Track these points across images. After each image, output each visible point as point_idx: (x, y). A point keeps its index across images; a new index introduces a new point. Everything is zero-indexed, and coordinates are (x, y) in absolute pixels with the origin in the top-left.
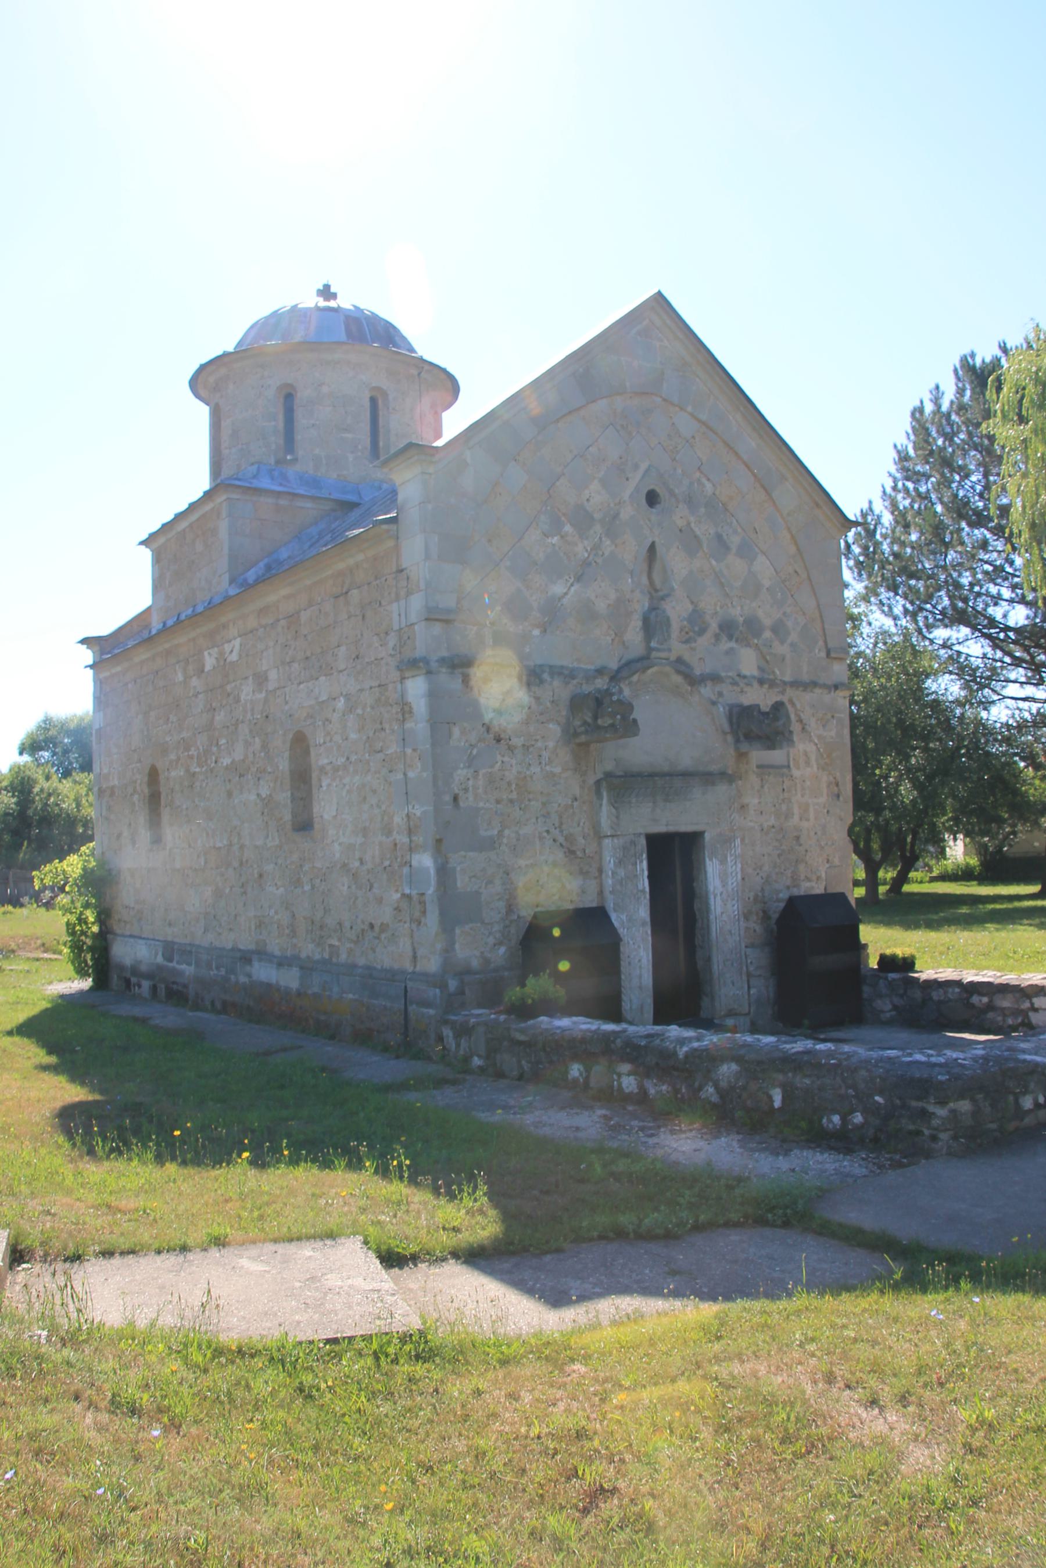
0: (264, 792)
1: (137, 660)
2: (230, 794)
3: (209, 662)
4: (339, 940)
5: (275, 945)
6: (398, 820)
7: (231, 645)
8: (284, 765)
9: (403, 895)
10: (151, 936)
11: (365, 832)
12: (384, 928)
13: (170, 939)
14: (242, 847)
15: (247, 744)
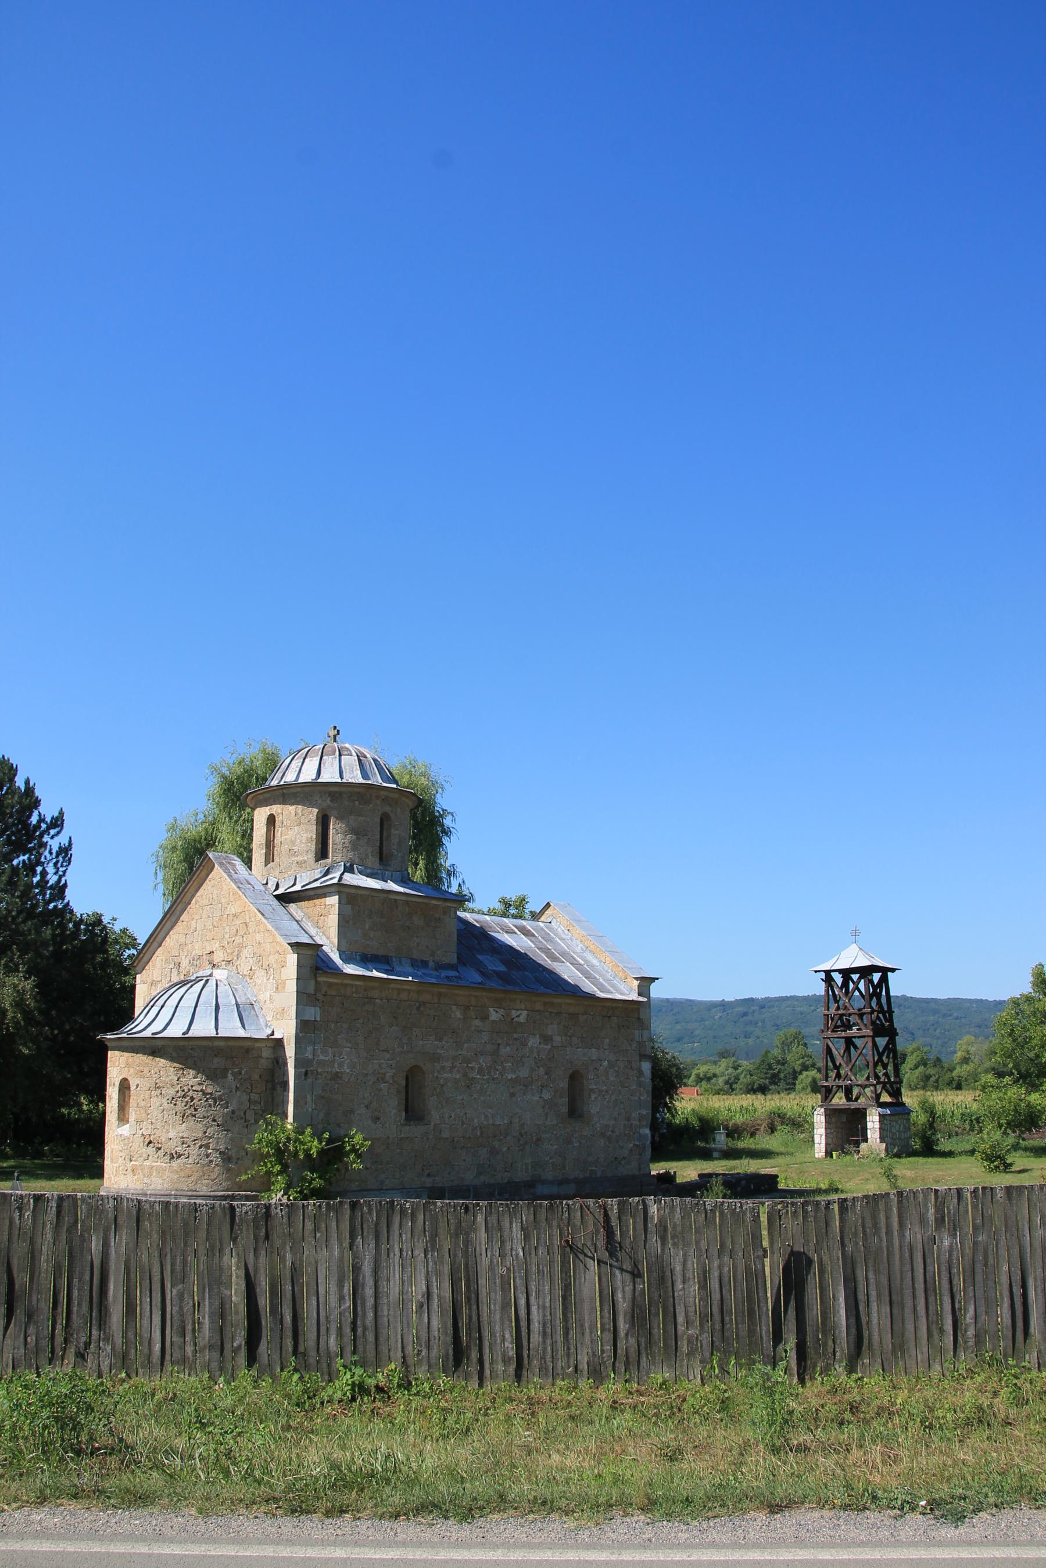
0: (547, 1096)
1: (392, 986)
2: (513, 1095)
3: (494, 1015)
4: (596, 1167)
5: (549, 1175)
6: (635, 1115)
7: (519, 1012)
8: (564, 1084)
9: (635, 1145)
10: (401, 1187)
11: (615, 1119)
12: (624, 1158)
13: (428, 1185)
14: (523, 1125)
15: (532, 1070)
